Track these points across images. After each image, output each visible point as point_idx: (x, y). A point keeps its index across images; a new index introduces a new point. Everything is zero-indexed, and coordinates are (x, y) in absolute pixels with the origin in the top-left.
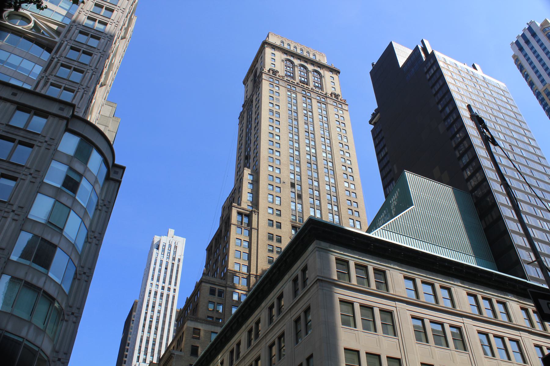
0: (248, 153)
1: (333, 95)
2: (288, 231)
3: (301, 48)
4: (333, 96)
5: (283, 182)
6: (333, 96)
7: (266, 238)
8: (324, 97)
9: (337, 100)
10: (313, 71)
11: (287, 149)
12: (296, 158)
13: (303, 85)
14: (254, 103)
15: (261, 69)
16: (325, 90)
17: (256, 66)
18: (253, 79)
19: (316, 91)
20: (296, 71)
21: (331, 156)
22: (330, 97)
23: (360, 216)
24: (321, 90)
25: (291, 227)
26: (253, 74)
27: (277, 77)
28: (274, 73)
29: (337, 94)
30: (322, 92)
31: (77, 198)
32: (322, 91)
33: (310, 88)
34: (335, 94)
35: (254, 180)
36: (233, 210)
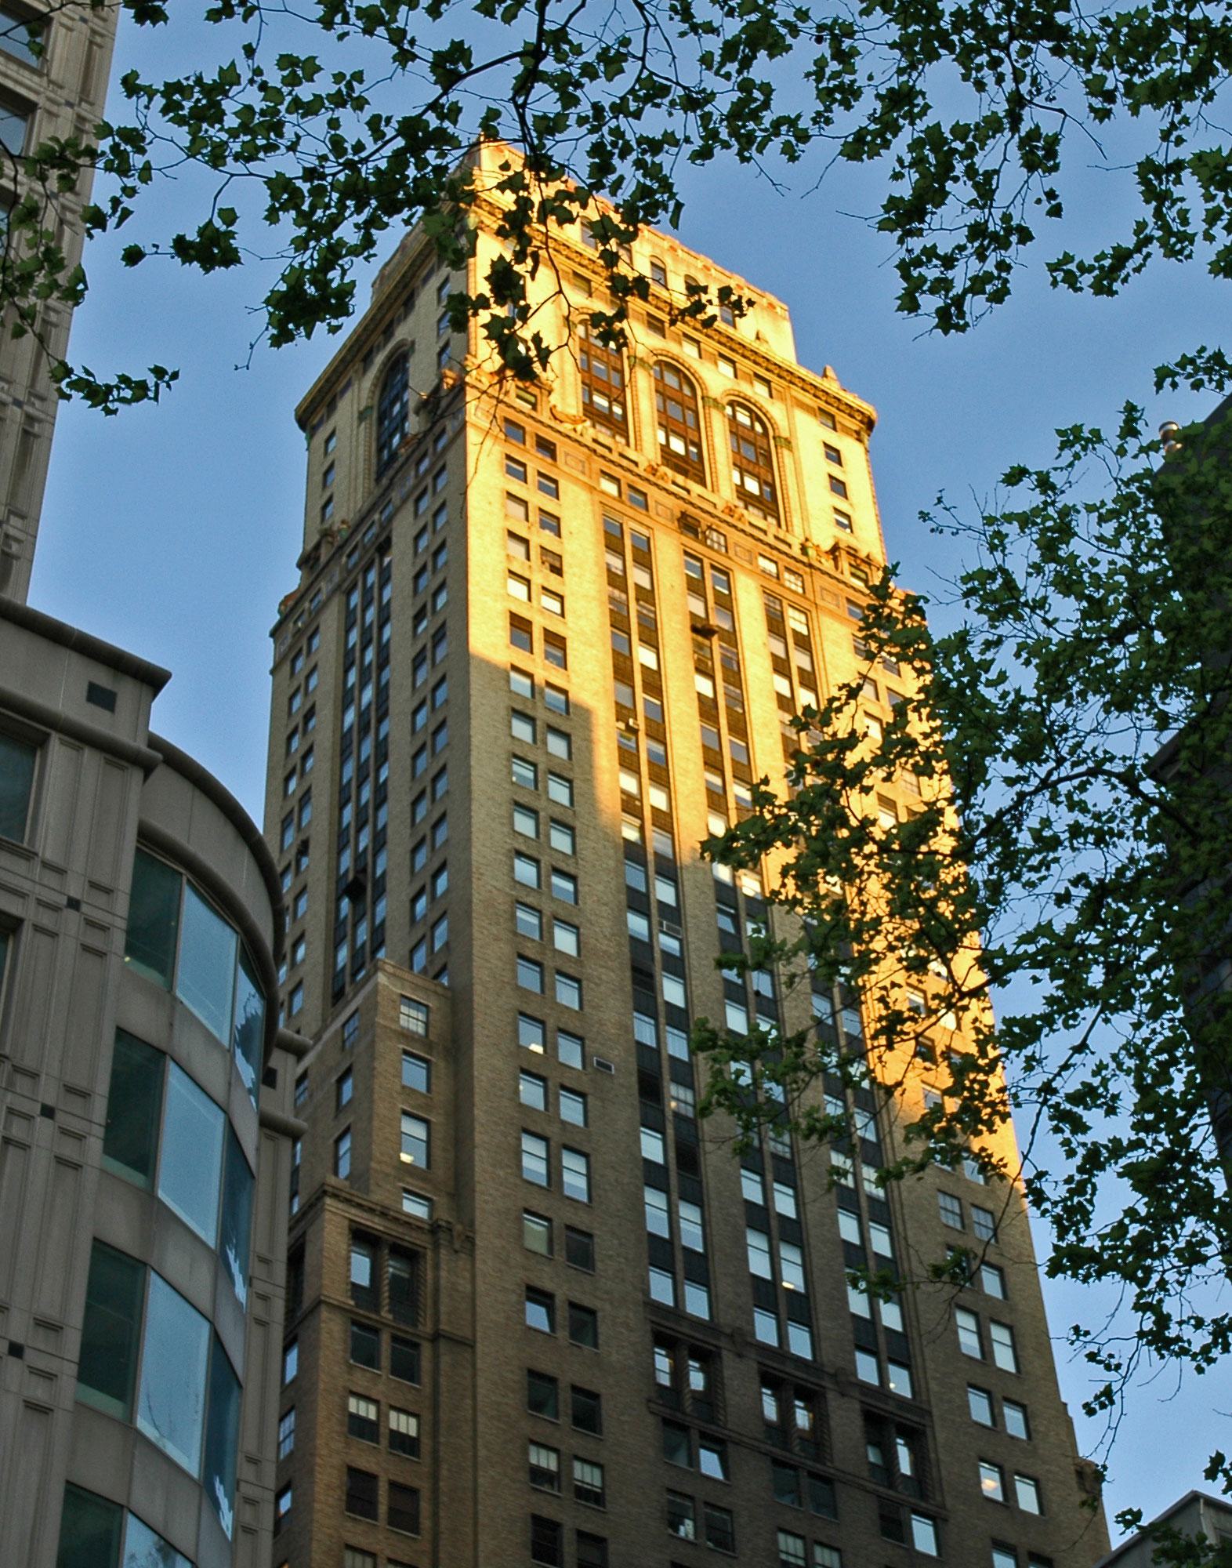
0: (358, 857)
1: (843, 553)
2: (632, 1363)
3: (657, 252)
4: (845, 563)
5: (599, 1063)
6: (845, 563)
7: (514, 1401)
8: (801, 569)
9: (533, 414)
10: (731, 404)
11: (612, 863)
12: (661, 925)
13: (680, 479)
14: (401, 559)
15: (440, 354)
16: (796, 521)
17: (401, 333)
18: (369, 408)
19: (751, 524)
20: (641, 395)
21: (531, 775)
22: (832, 572)
23: (1009, 1293)
24: (623, 441)
25: (649, 1338)
26: (377, 378)
27: (545, 417)
28: (857, 567)
29: (863, 554)
30: (781, 535)
31: (143, 1424)
32: (779, 525)
33: (643, 464)
34: (852, 552)
35: (432, 1037)
36: (327, 1216)
